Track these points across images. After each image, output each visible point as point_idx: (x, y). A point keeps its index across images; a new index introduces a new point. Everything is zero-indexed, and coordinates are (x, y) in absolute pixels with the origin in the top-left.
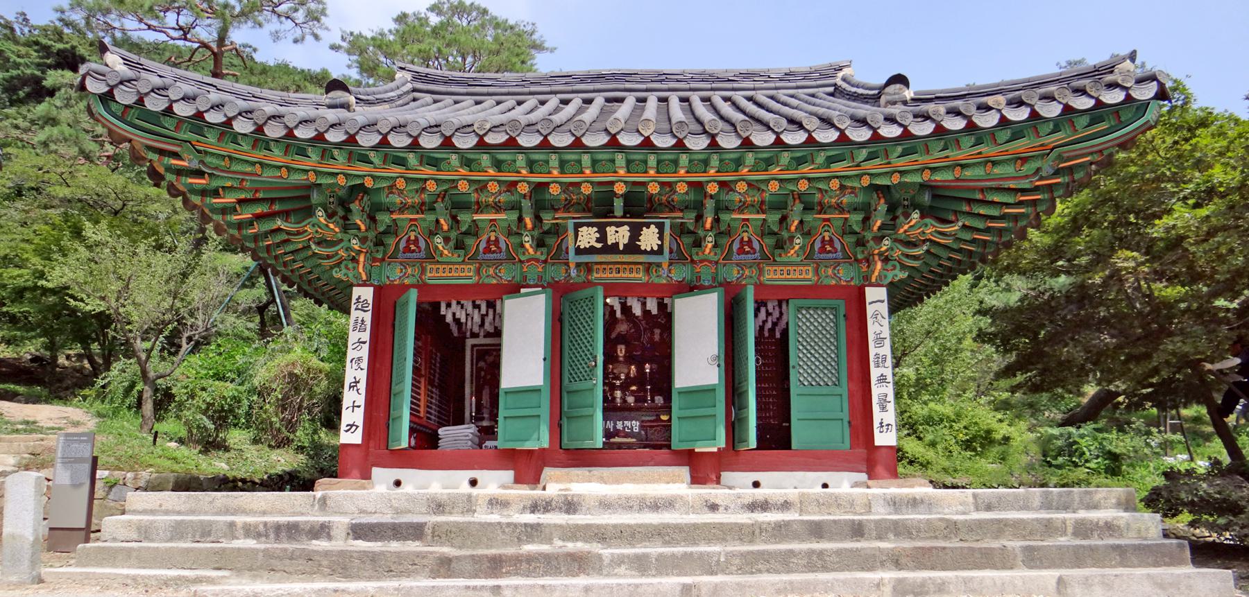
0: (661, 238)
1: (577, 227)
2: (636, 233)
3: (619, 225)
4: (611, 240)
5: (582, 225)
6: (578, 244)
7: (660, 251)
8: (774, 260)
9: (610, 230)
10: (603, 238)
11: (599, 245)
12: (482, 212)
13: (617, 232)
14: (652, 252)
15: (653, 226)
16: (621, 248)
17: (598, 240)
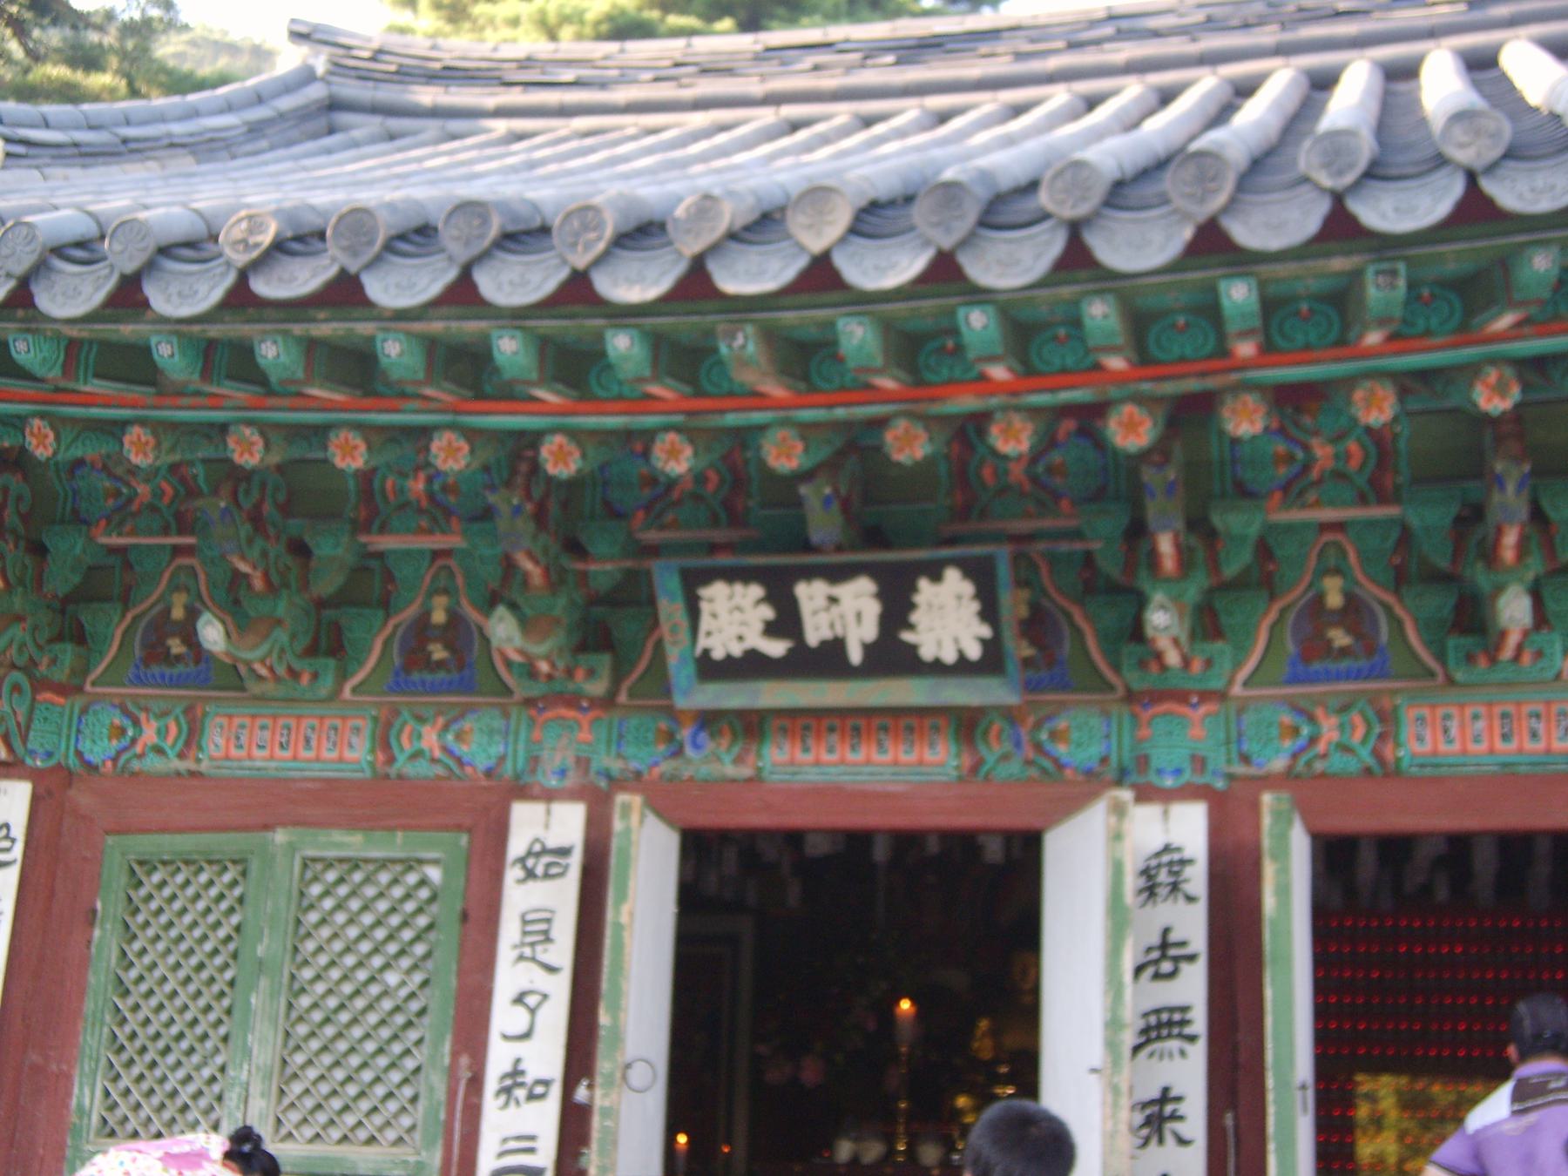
0: (989, 613)
1: (693, 581)
2: (897, 610)
3: (837, 574)
4: (816, 631)
5: (708, 576)
6: (703, 642)
7: (992, 661)
8: (1450, 681)
9: (811, 594)
10: (786, 622)
11: (776, 648)
12: (383, 530)
13: (833, 600)
14: (963, 667)
15: (952, 576)
16: (855, 655)
17: (771, 630)
